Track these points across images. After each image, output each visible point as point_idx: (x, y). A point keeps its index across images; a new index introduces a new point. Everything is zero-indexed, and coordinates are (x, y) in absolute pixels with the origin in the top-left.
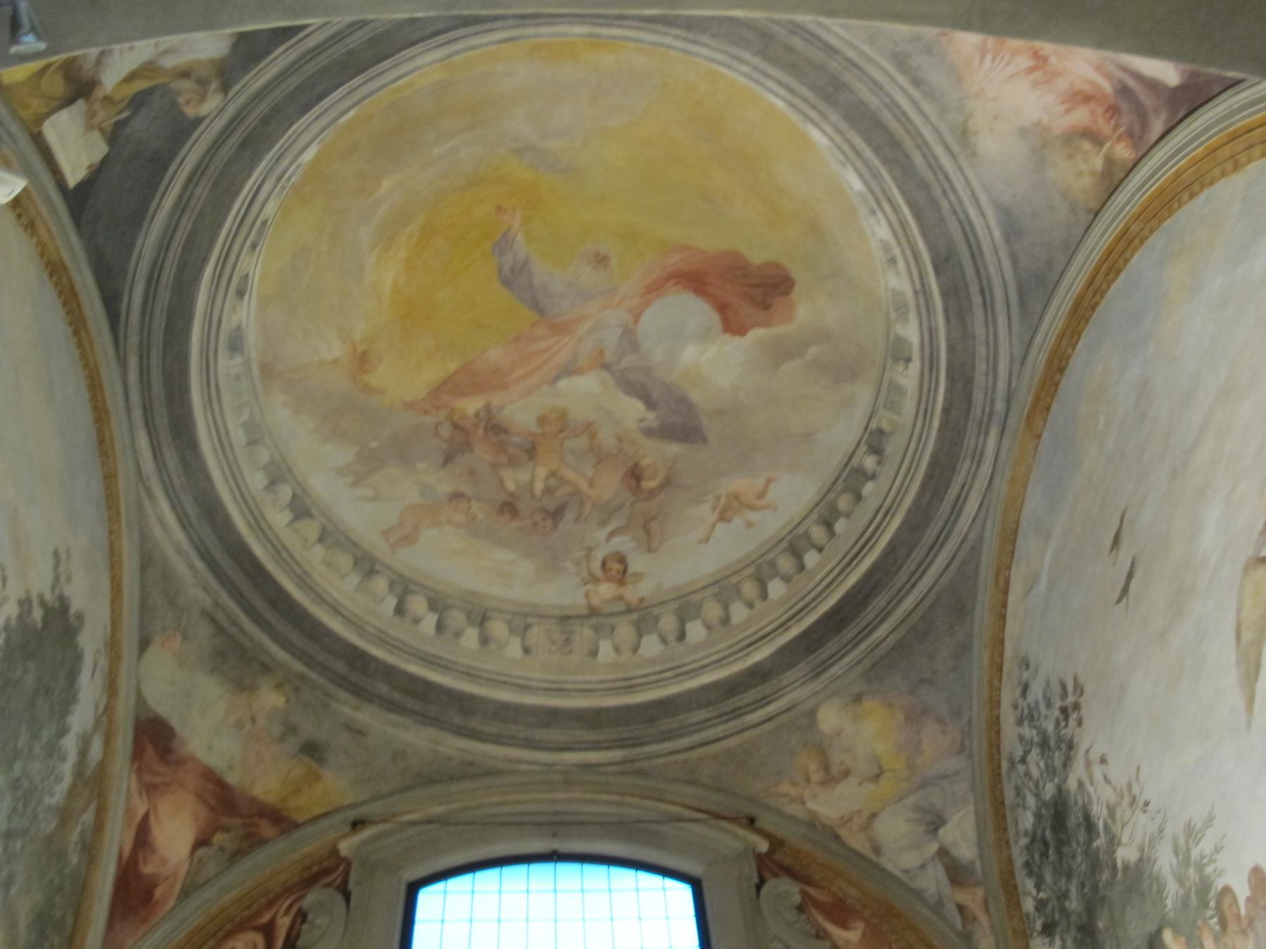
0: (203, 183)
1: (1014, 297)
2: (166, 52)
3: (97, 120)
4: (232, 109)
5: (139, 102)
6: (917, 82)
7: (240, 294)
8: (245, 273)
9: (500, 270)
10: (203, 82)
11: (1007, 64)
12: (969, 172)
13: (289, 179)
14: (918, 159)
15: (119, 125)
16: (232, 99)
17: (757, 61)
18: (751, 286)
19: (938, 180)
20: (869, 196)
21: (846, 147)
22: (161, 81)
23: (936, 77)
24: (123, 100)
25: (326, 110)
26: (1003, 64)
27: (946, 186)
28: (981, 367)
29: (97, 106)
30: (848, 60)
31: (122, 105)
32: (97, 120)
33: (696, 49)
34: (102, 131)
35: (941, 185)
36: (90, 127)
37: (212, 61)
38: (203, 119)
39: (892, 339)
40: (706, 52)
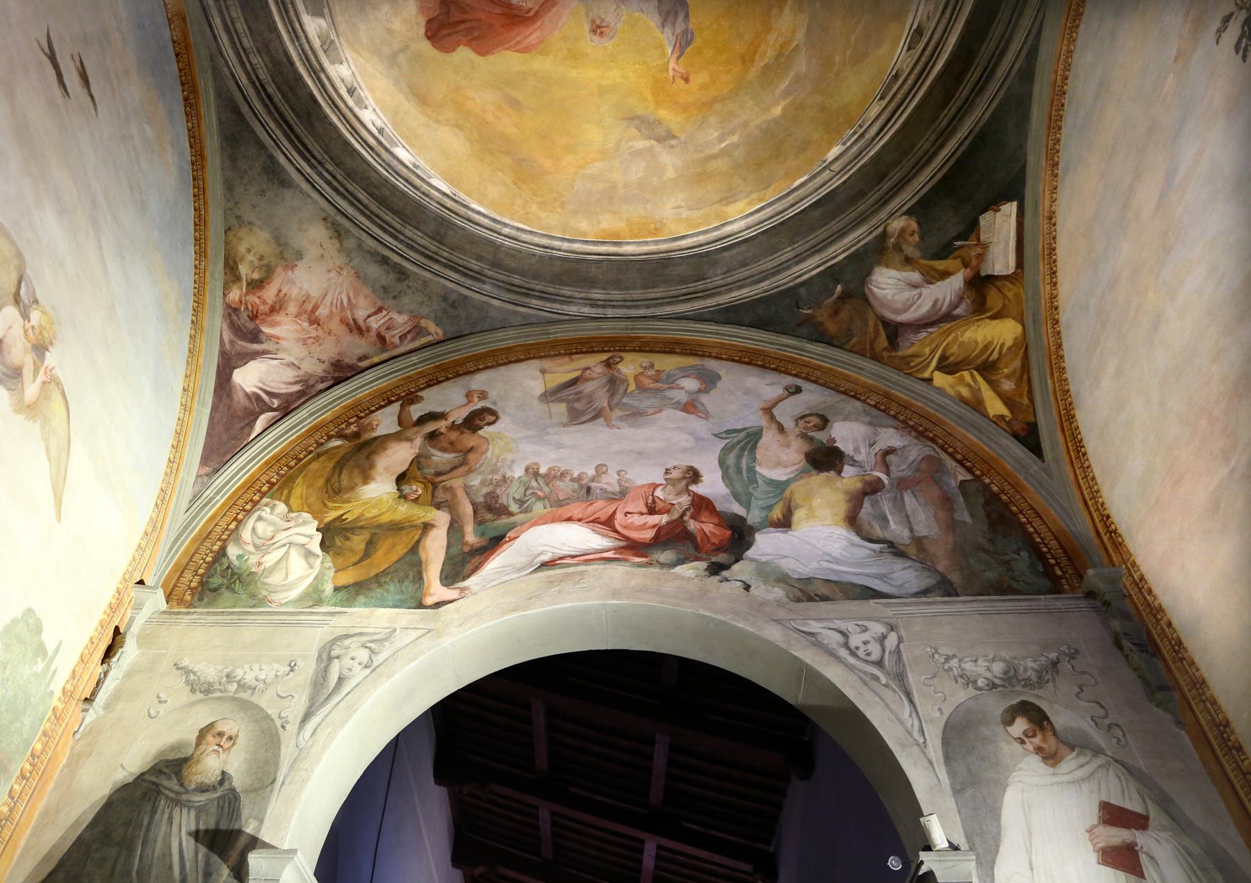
0: (920, 153)
1: (245, 109)
2: (916, 286)
3: (979, 250)
4: (883, 214)
5: (944, 251)
6: (385, 261)
7: (919, 32)
8: (910, 52)
9: (687, 16)
10: (898, 248)
11: (332, 304)
12: (323, 203)
13: (855, 133)
14: (362, 196)
15: (964, 236)
16: (881, 224)
17: (500, 240)
18: (463, 22)
19: (343, 186)
20: (388, 146)
21: (417, 182)
22: (925, 262)
23: (374, 271)
24: (955, 258)
25: (816, 190)
26: (335, 302)
27: (335, 184)
28: (241, 26)
29: (974, 263)
30: (437, 261)
31: (956, 254)
32: (979, 250)
33: (545, 241)
34: (979, 239)
35: (339, 182)
36: (985, 247)
37: (887, 266)
38: (904, 214)
39: (326, 11)
40: (537, 240)
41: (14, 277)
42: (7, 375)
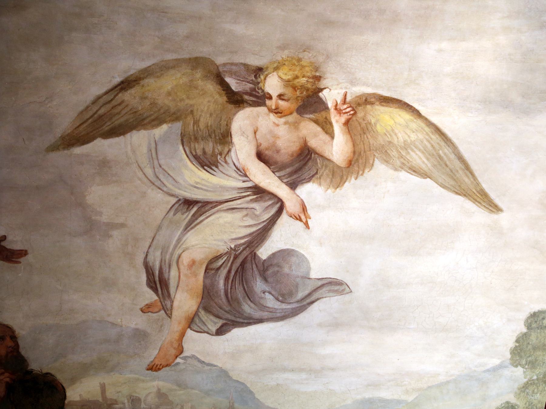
41: (211, 87)
42: (296, 172)
